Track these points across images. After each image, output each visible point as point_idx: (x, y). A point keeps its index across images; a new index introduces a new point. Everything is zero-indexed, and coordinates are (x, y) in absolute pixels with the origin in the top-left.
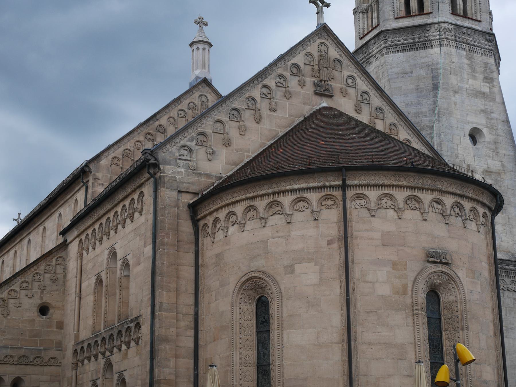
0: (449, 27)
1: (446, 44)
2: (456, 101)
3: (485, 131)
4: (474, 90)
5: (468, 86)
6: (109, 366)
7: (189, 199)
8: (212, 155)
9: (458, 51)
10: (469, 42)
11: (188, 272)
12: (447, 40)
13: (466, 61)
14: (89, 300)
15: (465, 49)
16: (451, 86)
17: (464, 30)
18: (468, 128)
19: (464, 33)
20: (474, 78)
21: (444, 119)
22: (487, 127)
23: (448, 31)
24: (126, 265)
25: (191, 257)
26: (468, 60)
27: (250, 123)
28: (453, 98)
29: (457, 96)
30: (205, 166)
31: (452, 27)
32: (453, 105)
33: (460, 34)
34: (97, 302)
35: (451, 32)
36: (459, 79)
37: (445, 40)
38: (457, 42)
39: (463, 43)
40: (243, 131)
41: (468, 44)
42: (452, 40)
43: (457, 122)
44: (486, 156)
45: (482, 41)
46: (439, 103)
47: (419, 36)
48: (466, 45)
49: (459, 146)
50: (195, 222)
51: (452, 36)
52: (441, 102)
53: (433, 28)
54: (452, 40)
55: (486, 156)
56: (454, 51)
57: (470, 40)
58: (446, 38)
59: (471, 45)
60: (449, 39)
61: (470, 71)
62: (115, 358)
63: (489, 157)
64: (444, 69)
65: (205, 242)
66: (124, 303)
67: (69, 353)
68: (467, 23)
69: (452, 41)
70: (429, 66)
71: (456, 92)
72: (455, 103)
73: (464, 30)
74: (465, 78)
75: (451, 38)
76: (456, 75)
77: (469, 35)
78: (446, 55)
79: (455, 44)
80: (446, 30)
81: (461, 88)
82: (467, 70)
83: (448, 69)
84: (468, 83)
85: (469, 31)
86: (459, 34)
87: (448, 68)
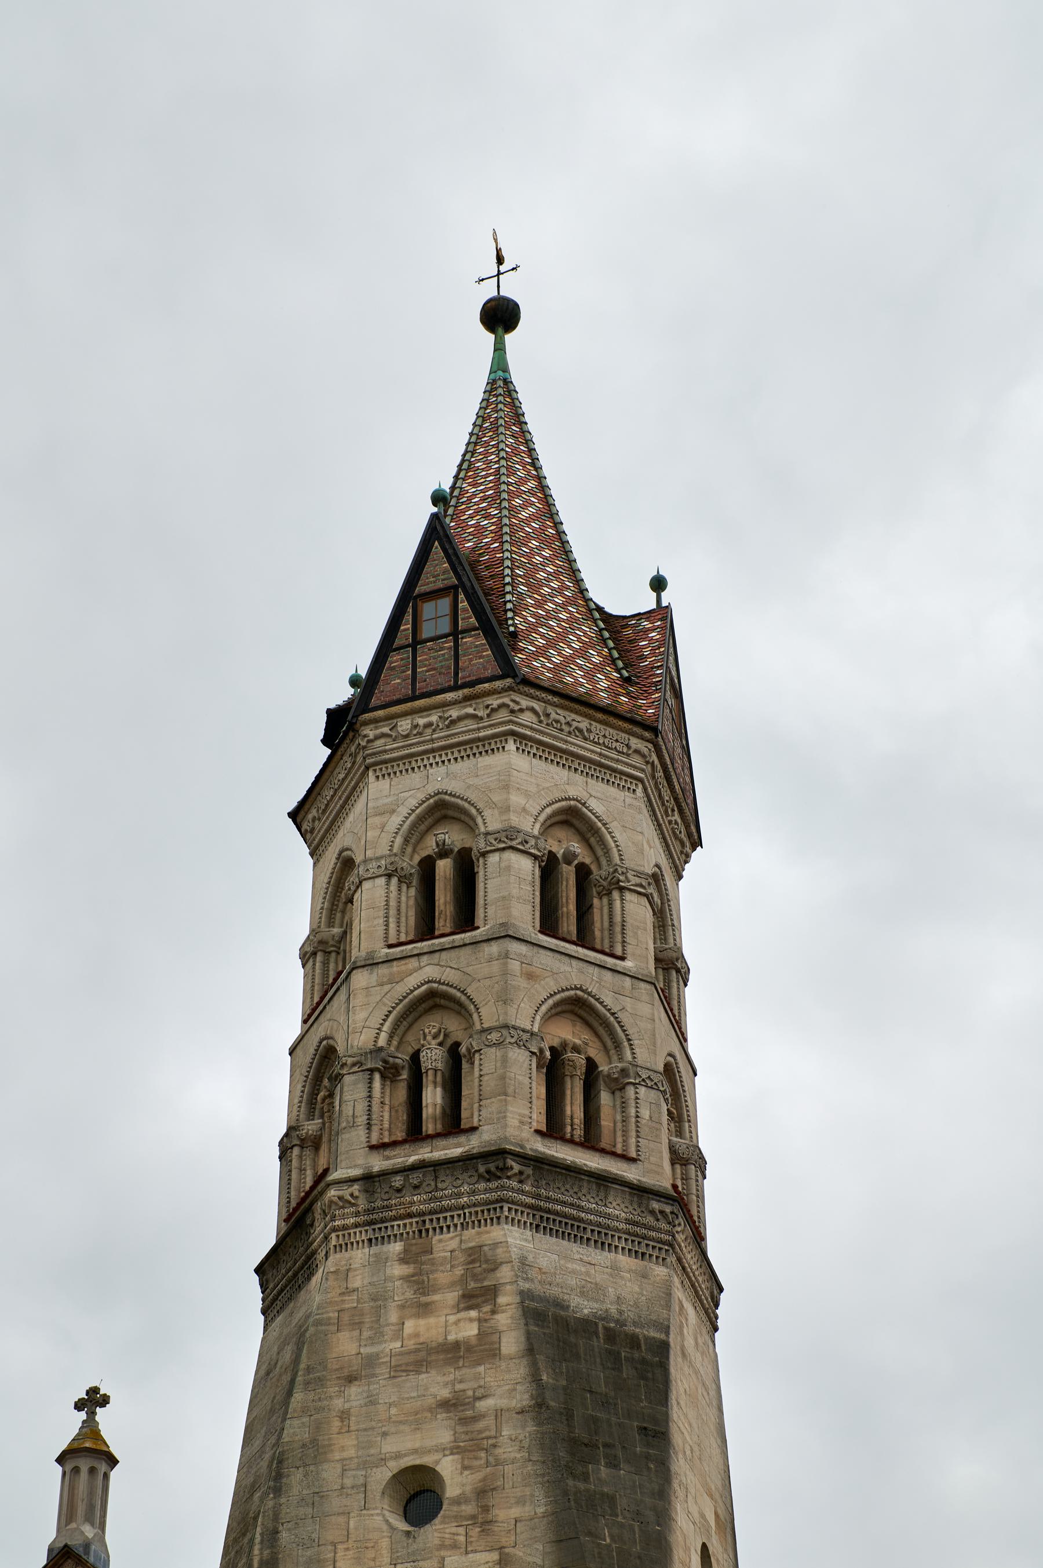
0: (340, 1193)
1: (335, 1246)
2: (346, 1406)
4: (417, 1351)
5: (398, 1344)
9: (374, 1249)
10: (414, 1209)
12: (340, 1233)
13: (398, 1270)
15: (402, 1234)
16: (335, 1367)
17: (398, 1181)
19: (399, 1191)
20: (424, 1309)
21: (295, 1479)
22: (455, 1449)
23: (343, 1207)
26: (407, 1263)
28: (338, 1403)
29: (354, 1391)
31: (356, 1188)
32: (336, 1423)
33: (386, 1197)
35: (353, 1205)
36: (366, 1334)
37: (333, 1235)
38: (374, 1224)
39: (395, 1219)
41: (410, 1216)
42: (356, 1225)
43: (344, 1470)
44: (442, 1546)
45: (466, 1188)
46: (286, 1438)
48: (407, 1221)
49: (340, 1547)
51: (357, 1214)
52: (296, 1430)
53: (317, 1216)
54: (356, 1225)
55: (442, 1546)
56: (359, 1256)
57: (418, 1201)
58: (334, 1230)
59: (422, 1214)
60: (345, 1228)
61: (409, 1294)
63: (454, 1546)
64: (318, 1323)
69: (358, 1230)
70: (300, 1327)
71: (351, 1379)
72: (344, 1416)
73: (398, 1181)
74: (388, 1325)
75: (352, 1220)
76: (357, 1325)
77: (416, 1187)
78: (331, 1277)
79: (370, 1232)
80: (336, 1204)
81: (371, 1361)
82: (403, 1292)
83: (329, 1318)
84: (399, 1334)
85: (415, 1178)
86: (383, 1200)
87: (331, 1315)
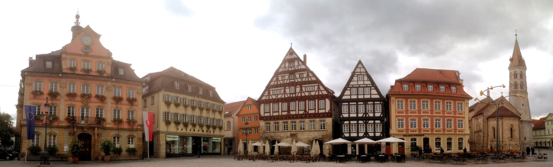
3: (524, 104)
6: (478, 134)
7: (487, 118)
8: (489, 112)
11: (487, 125)
14: (475, 126)
18: (522, 104)
24: (480, 123)
25: (487, 124)
27: (493, 108)
30: (488, 114)
34: (477, 127)
40: (493, 109)
47: (516, 92)
50: (487, 120)
62: (479, 133)
65: (488, 122)
66: (480, 127)
67: (473, 133)
68: (522, 90)
